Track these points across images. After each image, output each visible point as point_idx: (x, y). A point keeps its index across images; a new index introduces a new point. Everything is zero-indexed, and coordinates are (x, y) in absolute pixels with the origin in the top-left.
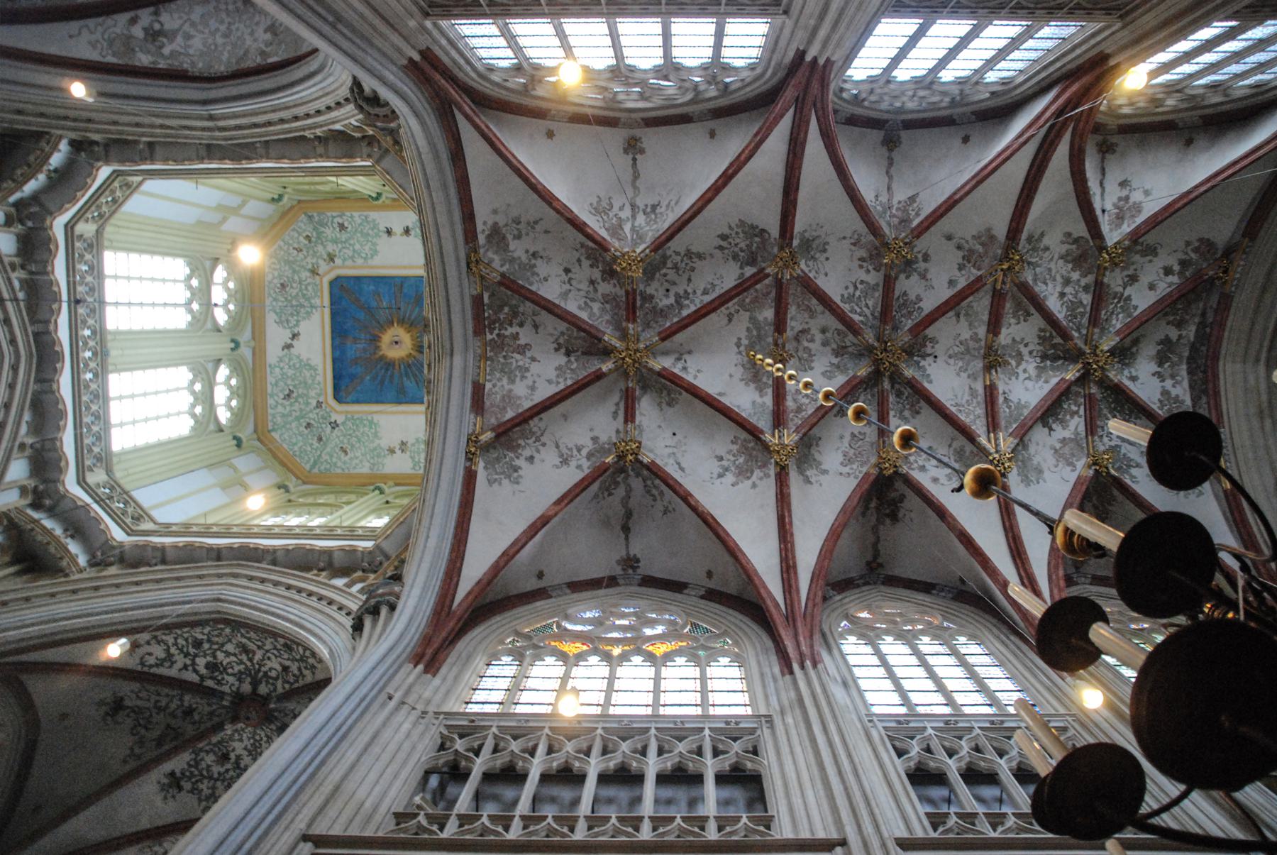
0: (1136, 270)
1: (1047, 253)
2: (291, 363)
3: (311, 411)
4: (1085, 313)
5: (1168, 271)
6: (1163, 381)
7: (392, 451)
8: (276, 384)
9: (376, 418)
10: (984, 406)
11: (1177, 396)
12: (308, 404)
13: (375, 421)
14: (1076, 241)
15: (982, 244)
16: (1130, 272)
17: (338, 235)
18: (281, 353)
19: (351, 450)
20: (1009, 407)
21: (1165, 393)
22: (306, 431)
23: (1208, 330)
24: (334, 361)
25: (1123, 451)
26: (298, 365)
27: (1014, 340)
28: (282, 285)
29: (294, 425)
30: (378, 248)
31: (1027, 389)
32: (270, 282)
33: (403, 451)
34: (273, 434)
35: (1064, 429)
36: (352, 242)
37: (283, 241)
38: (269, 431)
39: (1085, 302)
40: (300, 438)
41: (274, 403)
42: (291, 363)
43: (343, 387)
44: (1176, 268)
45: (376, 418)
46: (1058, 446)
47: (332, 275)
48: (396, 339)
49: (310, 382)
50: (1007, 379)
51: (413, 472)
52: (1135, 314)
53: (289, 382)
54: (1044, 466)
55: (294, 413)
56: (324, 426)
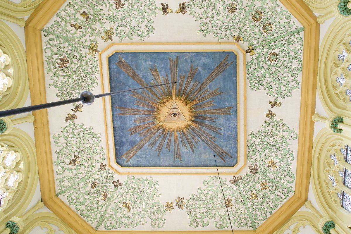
2: (75, 132)
3: (96, 172)
7: (170, 207)
8: (62, 153)
9: (155, 178)
12: (93, 166)
13: (154, 181)
17: (115, 14)
18: (65, 124)
19: (134, 206)
22: (92, 191)
24: (115, 129)
26: (82, 134)
28: (62, 60)
29: (81, 185)
30: (154, 25)
32: (49, 58)
33: (180, 207)
34: (61, 197)
36: (128, 19)
37: (60, 17)
38: (57, 195)
40: (86, 196)
41: (61, 169)
42: (75, 132)
43: (124, 153)
45: (155, 178)
47: (110, 52)
48: (174, 111)
49: (94, 148)
51: (191, 229)
53: (74, 149)
55: (80, 175)
56: (108, 185)
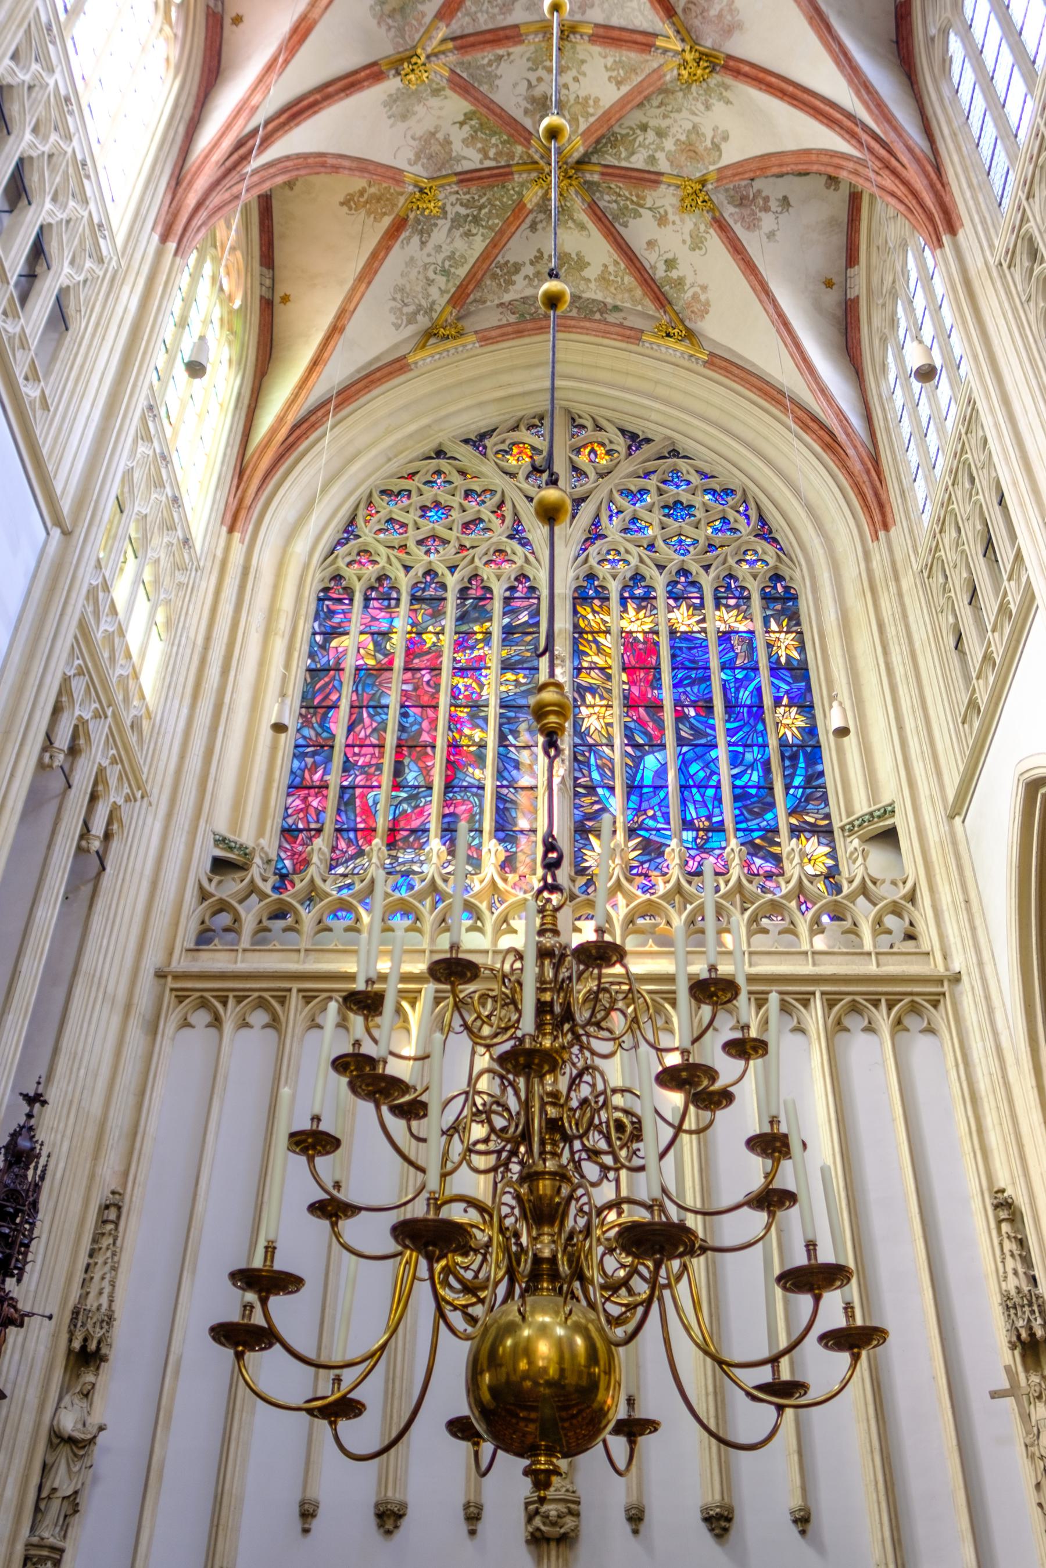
0: (674, 223)
1: (702, 108)
4: (619, 159)
5: (670, 264)
6: (532, 263)
10: (490, 26)
11: (513, 283)
14: (716, 147)
15: (720, 16)
16: (671, 217)
20: (490, 64)
21: (517, 268)
23: (597, 316)
25: (440, 222)
27: (583, 62)
31: (515, 85)
35: (464, 141)
39: (633, 159)
44: (674, 274)
46: (440, 136)
50: (528, 55)
52: (617, 225)
54: (412, 122)
